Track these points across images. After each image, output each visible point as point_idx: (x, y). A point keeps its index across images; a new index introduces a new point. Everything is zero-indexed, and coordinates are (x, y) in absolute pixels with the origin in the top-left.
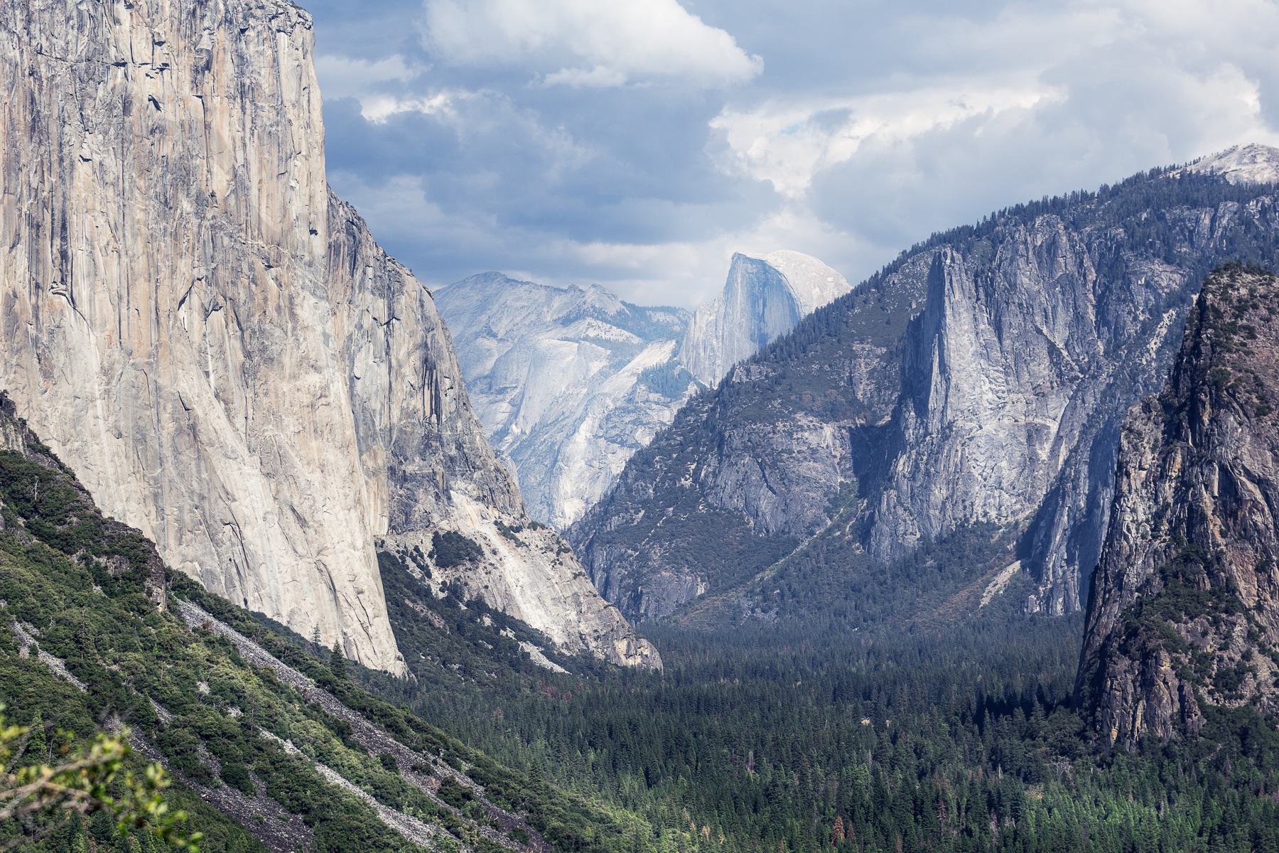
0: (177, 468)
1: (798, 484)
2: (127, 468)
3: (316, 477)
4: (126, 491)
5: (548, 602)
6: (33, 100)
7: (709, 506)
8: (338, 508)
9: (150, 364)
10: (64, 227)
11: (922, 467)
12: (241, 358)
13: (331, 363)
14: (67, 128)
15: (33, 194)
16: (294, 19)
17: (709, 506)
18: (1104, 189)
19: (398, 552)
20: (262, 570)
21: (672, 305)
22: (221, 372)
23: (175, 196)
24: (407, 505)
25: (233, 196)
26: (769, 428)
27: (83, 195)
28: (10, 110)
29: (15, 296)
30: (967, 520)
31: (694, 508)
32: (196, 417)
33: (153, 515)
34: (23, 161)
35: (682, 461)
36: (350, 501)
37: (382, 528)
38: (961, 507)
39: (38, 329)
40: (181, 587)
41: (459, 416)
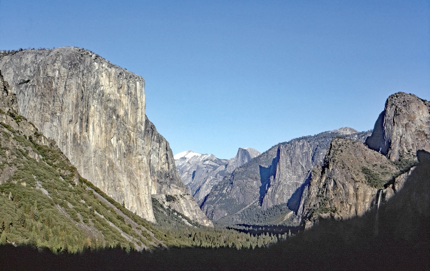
3: (138, 178)
4: (97, 178)
5: (190, 211)
9: (104, 151)
11: (274, 190)
14: (89, 99)
18: (315, 135)
22: (120, 154)
23: (112, 115)
28: (77, 94)
29: (76, 134)
32: (113, 163)
34: (79, 105)
35: (224, 187)
36: (146, 184)
37: (154, 192)
39: (80, 142)
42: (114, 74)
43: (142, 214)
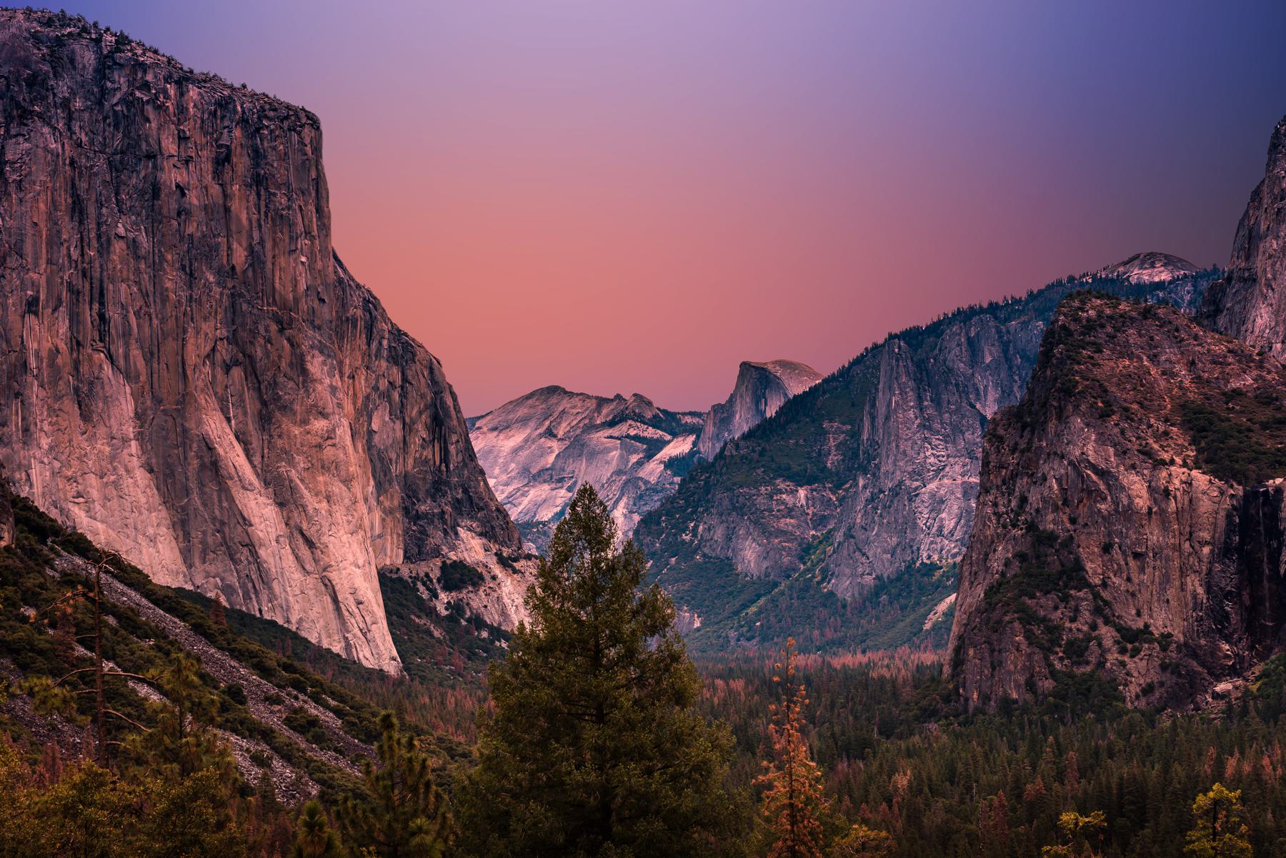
0: (201, 498)
1: (776, 537)
2: (157, 499)
4: (157, 518)
6: (73, 185)
7: (704, 555)
8: (342, 532)
10: (102, 294)
12: (258, 406)
13: (337, 410)
14: (104, 210)
15: (74, 265)
16: (304, 120)
17: (704, 555)
19: (410, 577)
20: (275, 585)
21: (698, 410)
24: (420, 539)
25: (251, 269)
26: (754, 491)
27: (119, 267)
28: (52, 194)
30: (914, 563)
31: (693, 558)
33: (181, 539)
34: (65, 236)
37: (394, 556)
38: (909, 551)
40: (70, 542)
41: (465, 465)
42: (195, 106)
43: (343, 644)
